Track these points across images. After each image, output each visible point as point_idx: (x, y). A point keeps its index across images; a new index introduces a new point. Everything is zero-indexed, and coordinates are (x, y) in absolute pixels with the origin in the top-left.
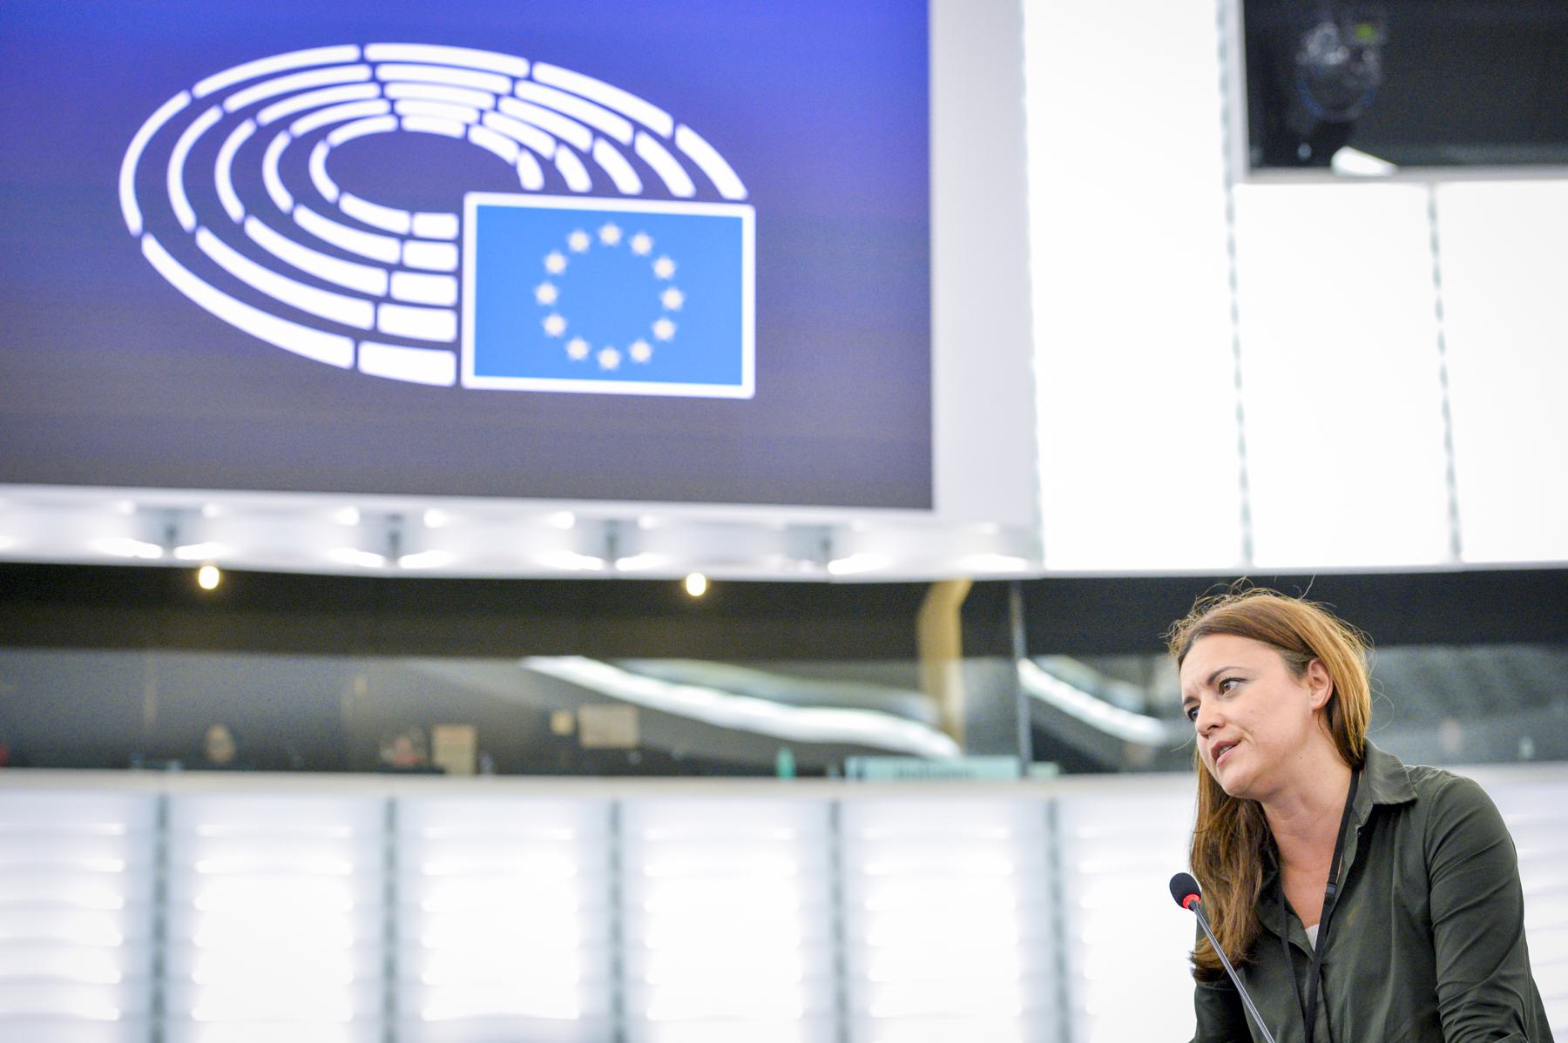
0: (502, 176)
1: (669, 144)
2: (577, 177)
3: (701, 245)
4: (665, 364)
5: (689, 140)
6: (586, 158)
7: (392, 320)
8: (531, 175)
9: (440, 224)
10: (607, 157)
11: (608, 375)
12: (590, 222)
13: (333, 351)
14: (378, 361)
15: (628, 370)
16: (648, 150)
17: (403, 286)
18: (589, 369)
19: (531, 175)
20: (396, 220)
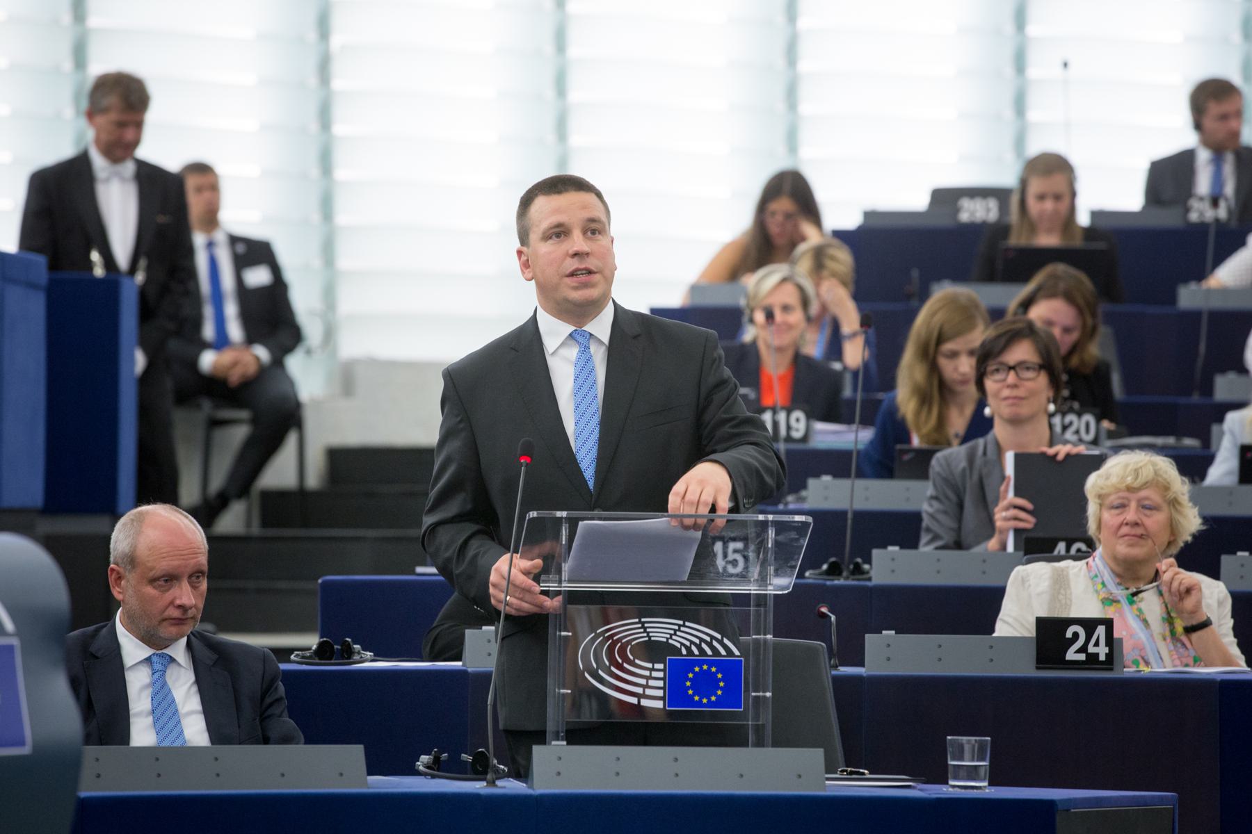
0: (677, 651)
1: (721, 642)
2: (696, 652)
3: (730, 668)
4: (717, 704)
5: (726, 641)
6: (699, 647)
7: (648, 692)
8: (684, 651)
9: (661, 666)
10: (704, 645)
11: (705, 703)
12: (700, 663)
13: (634, 700)
14: (644, 702)
15: (710, 704)
16: (715, 643)
17: (652, 683)
18: (700, 704)
19: (684, 651)
20: (650, 665)
